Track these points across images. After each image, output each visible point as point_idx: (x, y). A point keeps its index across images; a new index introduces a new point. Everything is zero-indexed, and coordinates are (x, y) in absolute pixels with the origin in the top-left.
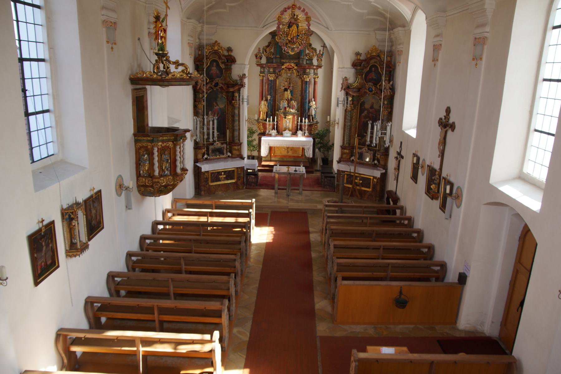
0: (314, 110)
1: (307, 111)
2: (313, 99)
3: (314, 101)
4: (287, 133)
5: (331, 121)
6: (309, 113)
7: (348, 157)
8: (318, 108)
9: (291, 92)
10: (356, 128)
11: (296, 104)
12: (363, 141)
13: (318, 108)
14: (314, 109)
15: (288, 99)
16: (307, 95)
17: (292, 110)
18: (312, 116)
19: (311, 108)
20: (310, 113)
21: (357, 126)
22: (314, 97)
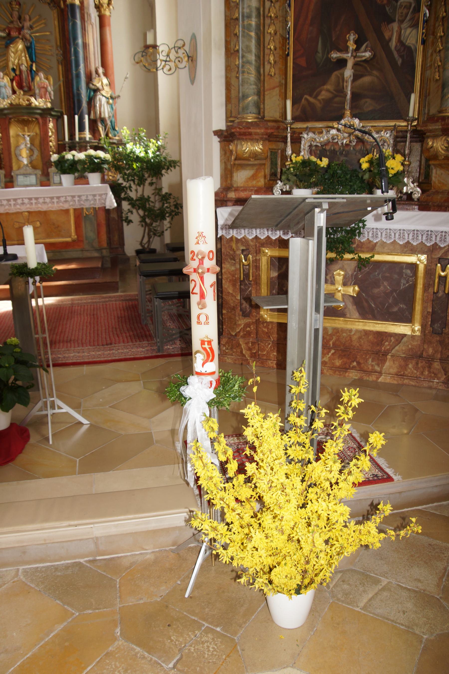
0: (108, 103)
1: (84, 105)
2: (101, 70)
3: (106, 74)
4: (25, 175)
5: (161, 49)
6: (92, 112)
7: (261, 182)
8: (119, 96)
9: (29, 49)
10: (285, 40)
11: (52, 82)
12: (324, 95)
13: (119, 96)
14: (107, 98)
15: (21, 71)
16: (81, 50)
17: (33, 99)
18: (103, 120)
19: (99, 97)
20: (95, 113)
21: (290, 24)
22: (104, 64)
